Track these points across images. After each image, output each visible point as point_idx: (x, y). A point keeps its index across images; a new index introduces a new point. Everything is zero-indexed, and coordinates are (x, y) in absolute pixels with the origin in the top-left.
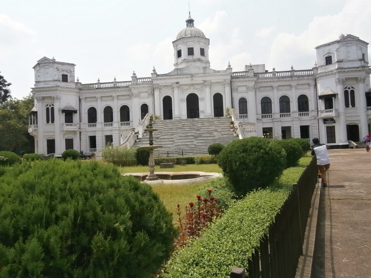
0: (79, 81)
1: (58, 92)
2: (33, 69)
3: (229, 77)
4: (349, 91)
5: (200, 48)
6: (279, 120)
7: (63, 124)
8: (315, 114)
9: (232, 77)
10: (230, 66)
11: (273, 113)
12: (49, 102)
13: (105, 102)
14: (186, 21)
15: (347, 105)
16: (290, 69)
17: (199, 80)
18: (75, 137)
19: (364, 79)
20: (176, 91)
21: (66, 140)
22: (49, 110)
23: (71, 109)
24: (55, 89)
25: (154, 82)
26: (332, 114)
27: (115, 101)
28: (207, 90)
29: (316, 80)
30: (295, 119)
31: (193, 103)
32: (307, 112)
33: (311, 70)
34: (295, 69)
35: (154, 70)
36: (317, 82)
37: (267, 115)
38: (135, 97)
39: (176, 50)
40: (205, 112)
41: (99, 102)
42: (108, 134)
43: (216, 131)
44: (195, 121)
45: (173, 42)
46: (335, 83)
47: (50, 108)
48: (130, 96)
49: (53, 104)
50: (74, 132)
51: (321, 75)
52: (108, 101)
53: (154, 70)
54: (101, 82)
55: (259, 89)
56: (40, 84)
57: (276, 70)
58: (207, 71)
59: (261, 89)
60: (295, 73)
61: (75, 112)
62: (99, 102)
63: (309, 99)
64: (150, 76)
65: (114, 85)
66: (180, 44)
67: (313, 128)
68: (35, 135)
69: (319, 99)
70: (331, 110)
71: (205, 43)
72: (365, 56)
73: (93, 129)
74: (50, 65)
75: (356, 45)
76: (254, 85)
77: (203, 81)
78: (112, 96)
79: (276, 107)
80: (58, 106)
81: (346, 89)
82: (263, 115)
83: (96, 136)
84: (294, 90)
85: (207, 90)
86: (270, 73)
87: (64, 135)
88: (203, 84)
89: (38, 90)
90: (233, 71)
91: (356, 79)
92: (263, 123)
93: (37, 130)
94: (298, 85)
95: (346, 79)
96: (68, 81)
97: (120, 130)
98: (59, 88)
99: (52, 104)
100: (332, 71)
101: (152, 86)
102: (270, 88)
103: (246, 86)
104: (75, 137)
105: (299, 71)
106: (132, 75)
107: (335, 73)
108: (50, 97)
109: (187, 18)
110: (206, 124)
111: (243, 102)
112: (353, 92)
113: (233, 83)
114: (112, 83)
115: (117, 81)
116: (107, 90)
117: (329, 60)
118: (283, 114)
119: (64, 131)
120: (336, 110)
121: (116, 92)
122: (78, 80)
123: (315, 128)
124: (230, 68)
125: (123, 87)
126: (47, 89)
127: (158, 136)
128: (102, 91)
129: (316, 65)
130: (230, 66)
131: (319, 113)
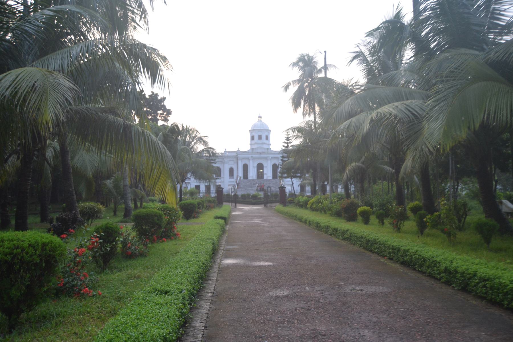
17: (265, 156)
20: (251, 162)
28: (269, 162)
45: (250, 131)
85: (269, 162)
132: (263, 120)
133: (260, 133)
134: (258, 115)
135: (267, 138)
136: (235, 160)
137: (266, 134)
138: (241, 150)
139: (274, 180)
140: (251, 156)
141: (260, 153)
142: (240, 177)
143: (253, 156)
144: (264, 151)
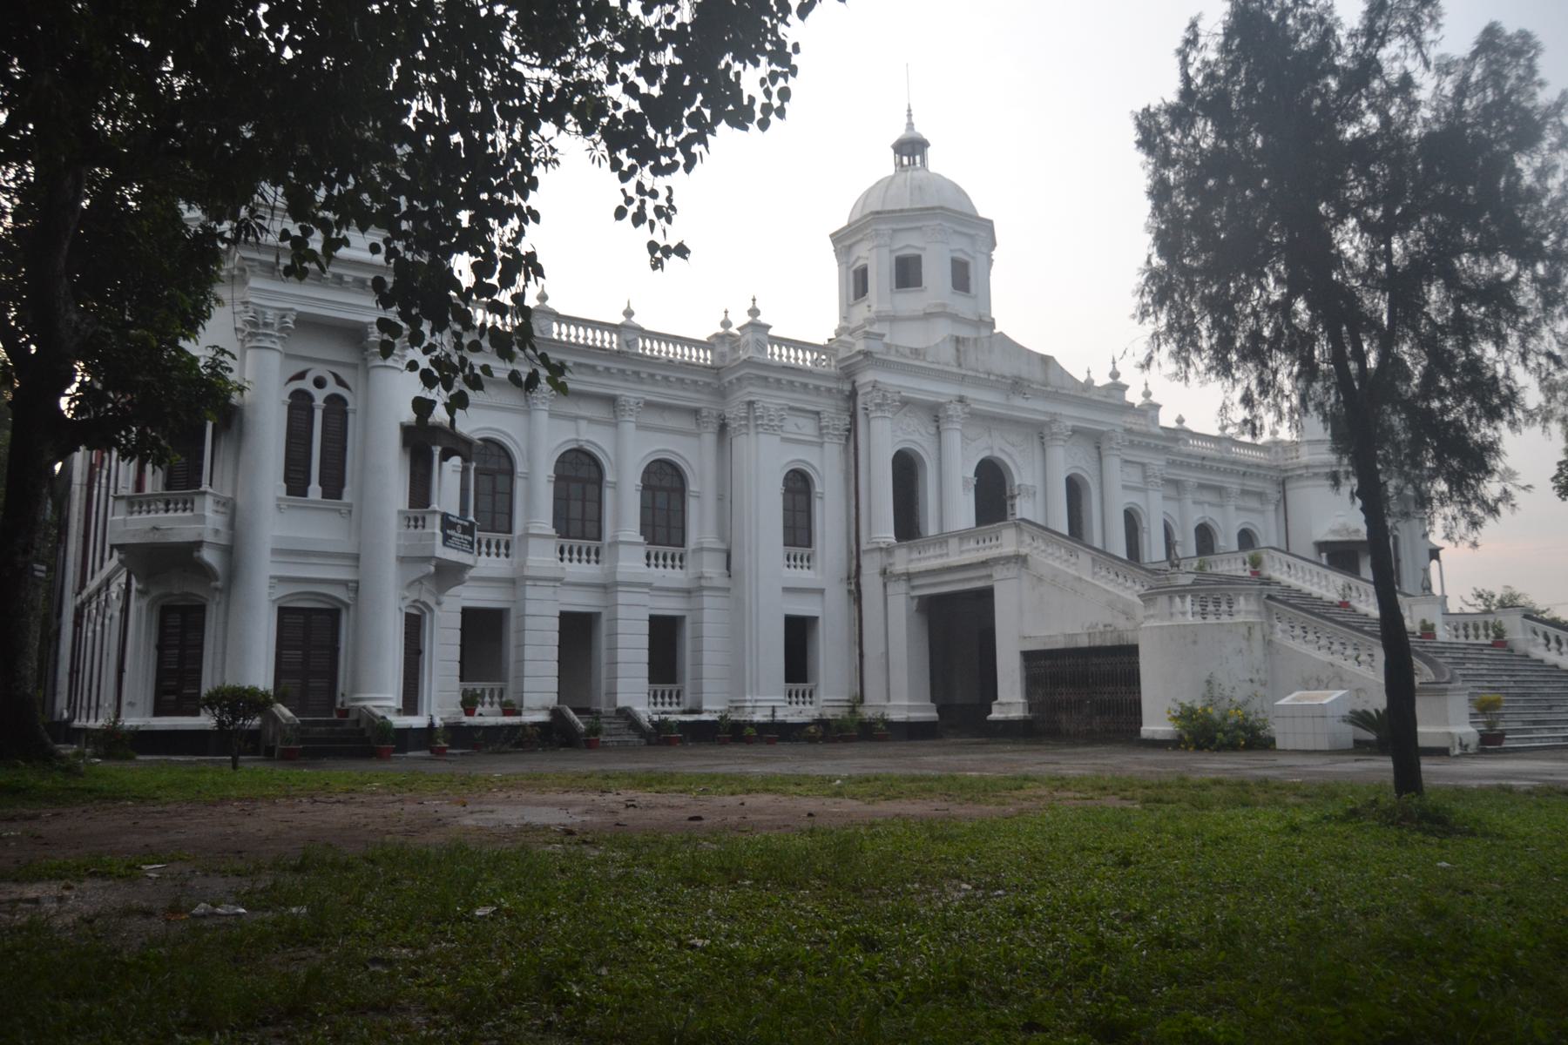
12: (326, 355)
22: (311, 411)
27: (628, 427)
29: (1283, 484)
36: (1290, 494)
38: (771, 429)
39: (885, 251)
42: (580, 602)
47: (319, 397)
49: (344, 374)
52: (583, 424)
66: (919, 228)
77: (1046, 413)
78: (611, 401)
83: (530, 608)
94: (1244, 493)
99: (335, 375)
101: (840, 391)
103: (1143, 465)
116: (601, 364)
121: (641, 381)
125: (670, 364)
134: (899, 132)
136: (830, 408)
141: (1017, 385)
143: (970, 393)
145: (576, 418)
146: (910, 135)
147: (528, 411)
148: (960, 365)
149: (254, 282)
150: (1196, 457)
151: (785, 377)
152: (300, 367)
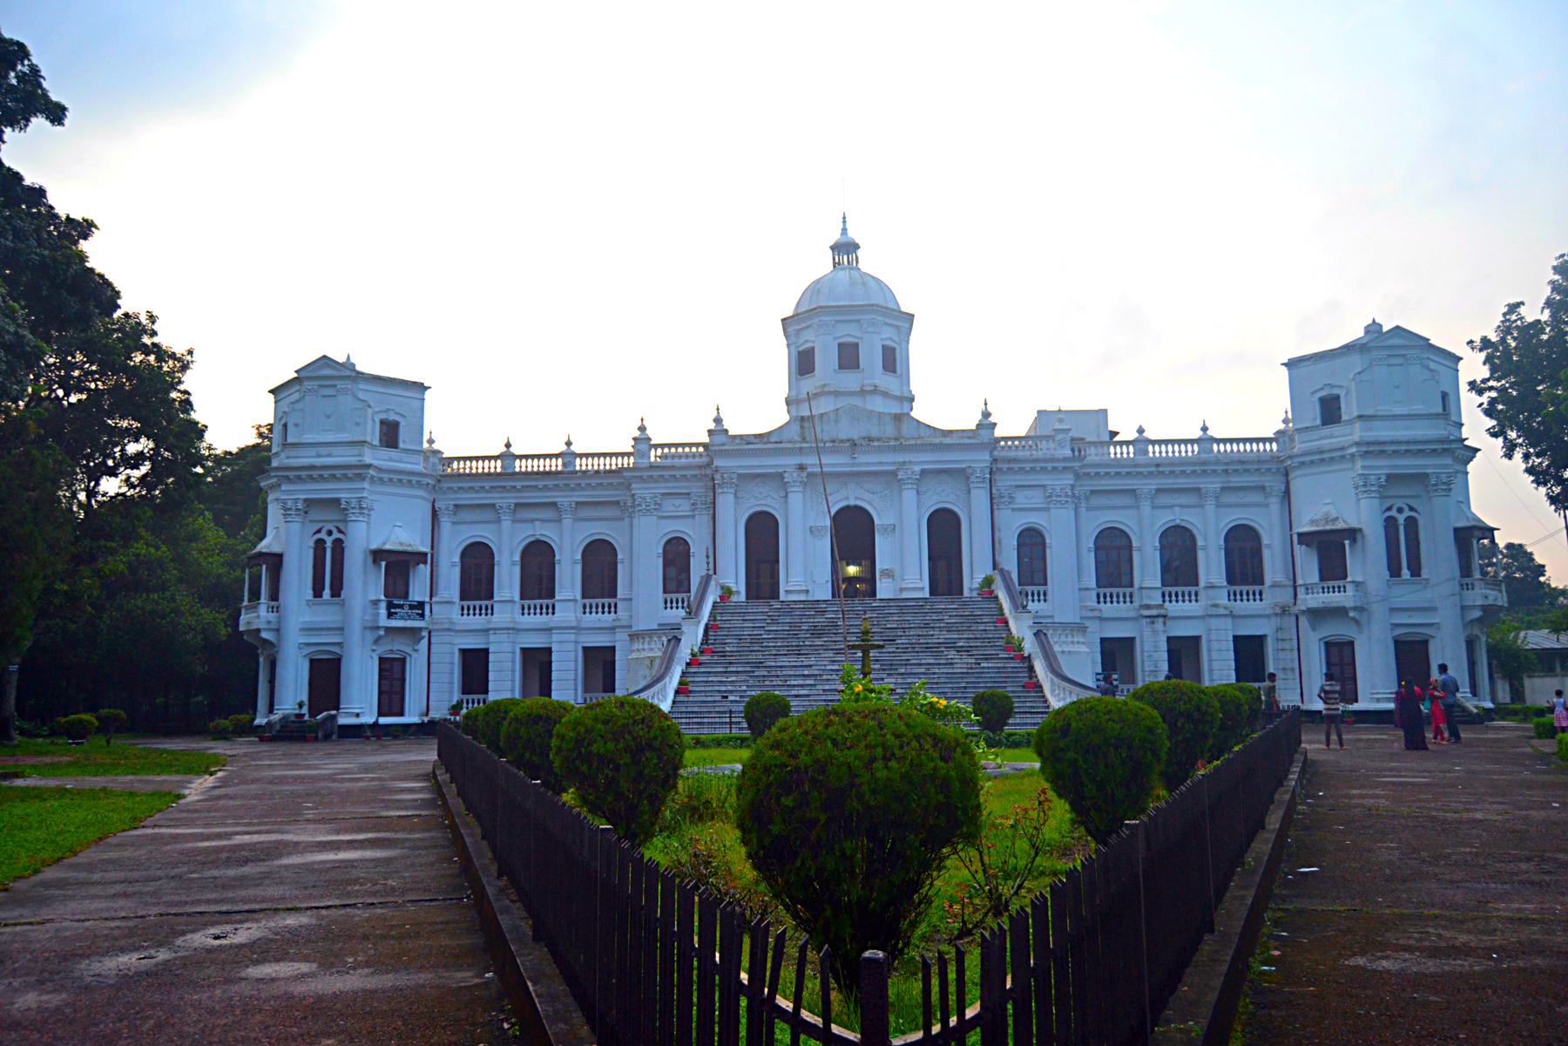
0: (435, 446)
1: (366, 485)
2: (271, 396)
3: (987, 457)
4: (1401, 519)
5: (884, 347)
6: (1162, 612)
7: (376, 603)
8: (1285, 597)
9: (995, 460)
10: (986, 415)
11: (1136, 585)
13: (529, 525)
14: (833, 248)
15: (1395, 571)
16: (1198, 434)
18: (414, 655)
19: (1448, 483)
20: (796, 499)
21: (381, 660)
22: (324, 550)
23: (409, 549)
24: (358, 472)
25: (718, 462)
26: (1344, 598)
27: (567, 522)
28: (909, 495)
29: (1287, 475)
30: (1214, 611)
31: (853, 535)
32: (1257, 588)
33: (1270, 440)
34: (1214, 432)
35: (718, 420)
36: (1292, 484)
37: (1114, 591)
40: (897, 574)
41: (506, 524)
43: (950, 645)
44: (874, 609)
46: (1353, 492)
48: (623, 509)
50: (414, 632)
51: (1307, 459)
52: (538, 524)
53: (718, 420)
54: (515, 450)
55: (1087, 499)
56: (301, 452)
57: (1148, 434)
58: (906, 430)
59: (1094, 501)
60: (1215, 447)
61: (421, 557)
62: (506, 524)
63: (1265, 541)
64: (706, 439)
65: (564, 465)
67: (1281, 645)
68: (266, 641)
69: (1300, 543)
70: (1341, 583)
71: (897, 327)
72: (1452, 398)
73: (477, 621)
74: (340, 384)
75: (1423, 366)
76: (1072, 486)
78: (554, 504)
79: (1147, 569)
80: (364, 537)
81: (1389, 514)
82: (1102, 591)
84: (1210, 507)
85: (909, 495)
86: (1127, 443)
87: (377, 641)
88: (894, 473)
89: (291, 474)
90: (998, 433)
91: (1421, 478)
92: (1101, 619)
93: (279, 621)
95: (1389, 477)
96: (401, 445)
97: (577, 629)
98: (371, 472)
100: (1343, 449)
102: (1127, 500)
104: (414, 655)
105: (1231, 441)
106: (637, 434)
107: (1353, 455)
108: (337, 501)
109: (835, 237)
110: (913, 619)
111: (1032, 544)
112: (1412, 523)
113: (997, 477)
114: (557, 456)
115: (575, 448)
116: (540, 484)
117: (1330, 410)
118: (1173, 589)
119: (378, 628)
120: (1357, 584)
121: (573, 489)
122: (431, 441)
123: (1287, 645)
124: (986, 424)
126: (326, 473)
127: (753, 657)
128: (519, 484)
129: (1285, 421)
130: (986, 415)
131: (1301, 591)
132: (868, 262)
133: (848, 333)
135: (893, 361)
136: (697, 489)
137: (887, 335)
138: (737, 426)
139: (942, 603)
140: (794, 460)
142: (726, 594)
143: (810, 460)
144: (874, 433)
145: (533, 521)
146: (844, 240)
147: (499, 521)
148: (804, 440)
149: (284, 487)
150: (1147, 465)
151: (655, 473)
152: (316, 527)
